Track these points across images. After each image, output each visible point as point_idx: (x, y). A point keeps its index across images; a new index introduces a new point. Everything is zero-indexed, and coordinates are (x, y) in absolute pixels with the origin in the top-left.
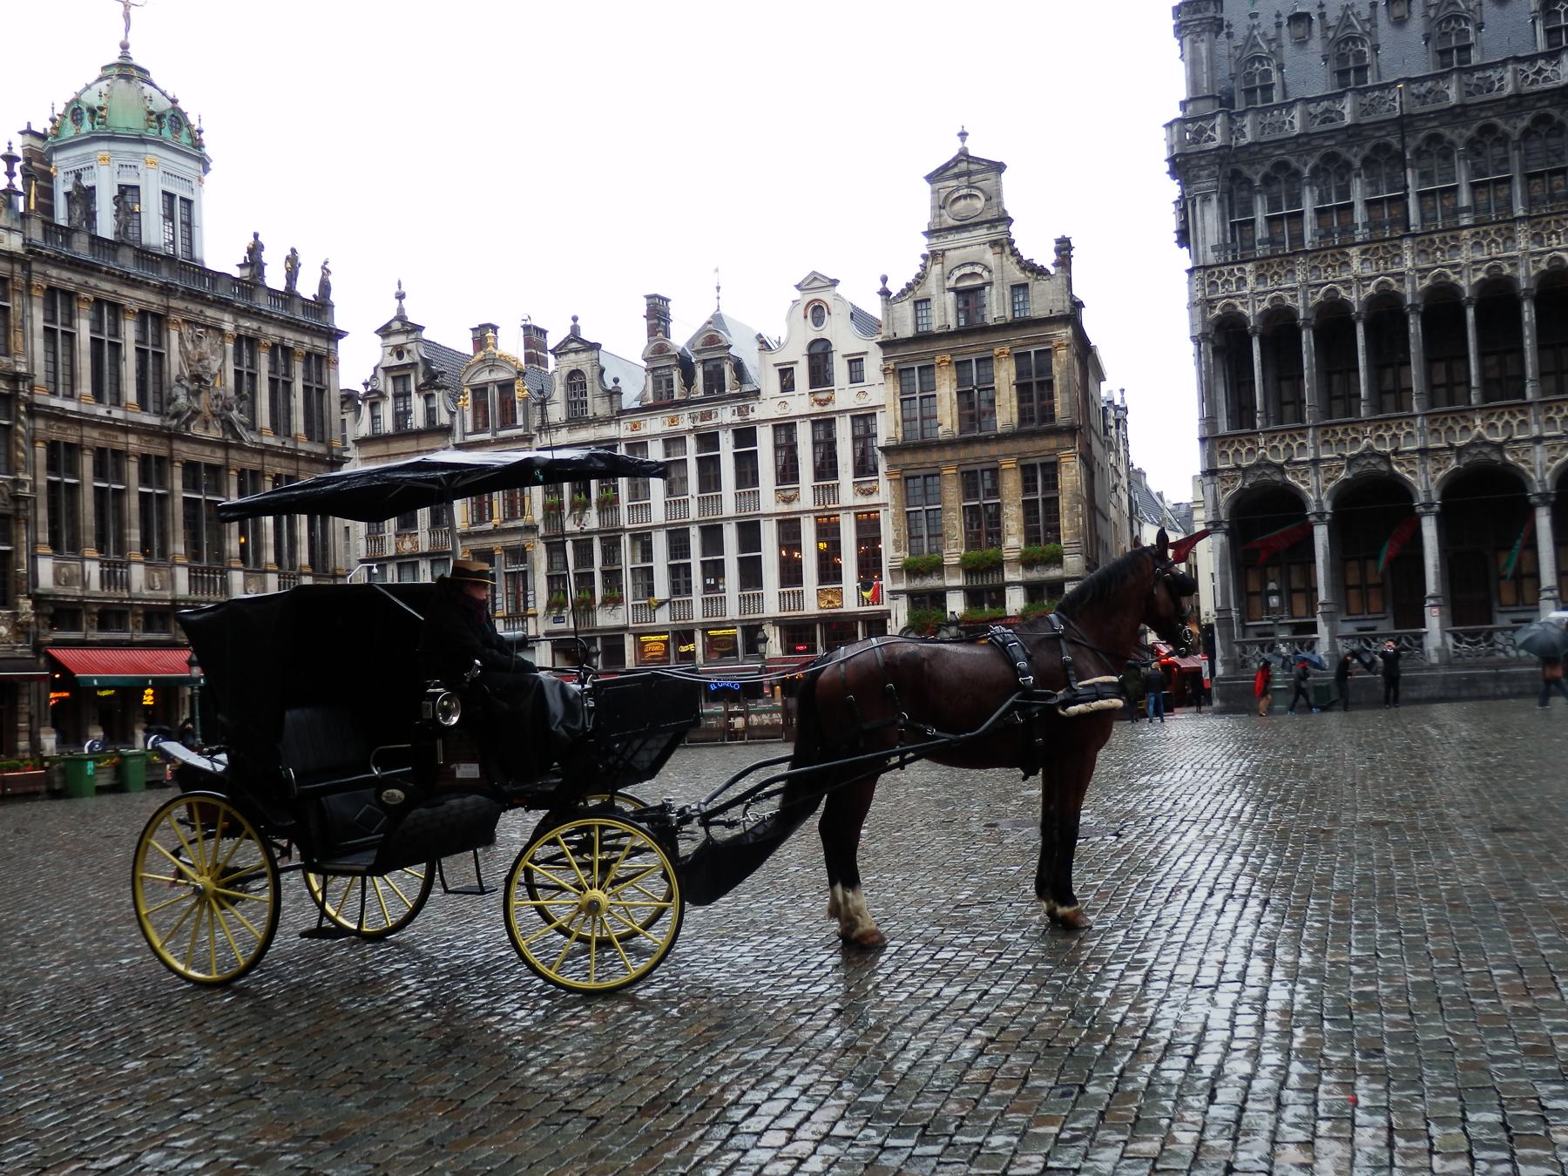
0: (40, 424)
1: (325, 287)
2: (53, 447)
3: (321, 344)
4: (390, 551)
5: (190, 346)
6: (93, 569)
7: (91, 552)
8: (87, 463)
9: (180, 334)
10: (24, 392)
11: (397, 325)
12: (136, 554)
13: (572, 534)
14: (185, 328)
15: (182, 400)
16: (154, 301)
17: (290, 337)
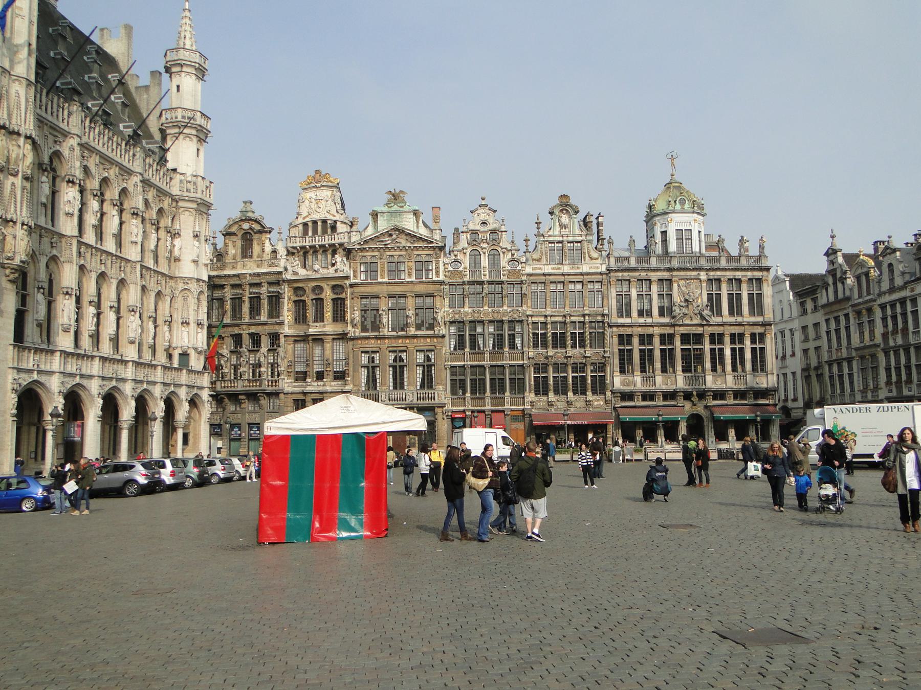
0: (615, 329)
1: (762, 247)
2: (621, 337)
3: (758, 274)
4: (834, 357)
5: (684, 289)
7: (638, 373)
8: (636, 340)
9: (679, 285)
10: (606, 320)
11: (830, 251)
12: (658, 372)
13: (891, 348)
14: (682, 282)
15: (678, 311)
16: (666, 275)
17: (739, 274)
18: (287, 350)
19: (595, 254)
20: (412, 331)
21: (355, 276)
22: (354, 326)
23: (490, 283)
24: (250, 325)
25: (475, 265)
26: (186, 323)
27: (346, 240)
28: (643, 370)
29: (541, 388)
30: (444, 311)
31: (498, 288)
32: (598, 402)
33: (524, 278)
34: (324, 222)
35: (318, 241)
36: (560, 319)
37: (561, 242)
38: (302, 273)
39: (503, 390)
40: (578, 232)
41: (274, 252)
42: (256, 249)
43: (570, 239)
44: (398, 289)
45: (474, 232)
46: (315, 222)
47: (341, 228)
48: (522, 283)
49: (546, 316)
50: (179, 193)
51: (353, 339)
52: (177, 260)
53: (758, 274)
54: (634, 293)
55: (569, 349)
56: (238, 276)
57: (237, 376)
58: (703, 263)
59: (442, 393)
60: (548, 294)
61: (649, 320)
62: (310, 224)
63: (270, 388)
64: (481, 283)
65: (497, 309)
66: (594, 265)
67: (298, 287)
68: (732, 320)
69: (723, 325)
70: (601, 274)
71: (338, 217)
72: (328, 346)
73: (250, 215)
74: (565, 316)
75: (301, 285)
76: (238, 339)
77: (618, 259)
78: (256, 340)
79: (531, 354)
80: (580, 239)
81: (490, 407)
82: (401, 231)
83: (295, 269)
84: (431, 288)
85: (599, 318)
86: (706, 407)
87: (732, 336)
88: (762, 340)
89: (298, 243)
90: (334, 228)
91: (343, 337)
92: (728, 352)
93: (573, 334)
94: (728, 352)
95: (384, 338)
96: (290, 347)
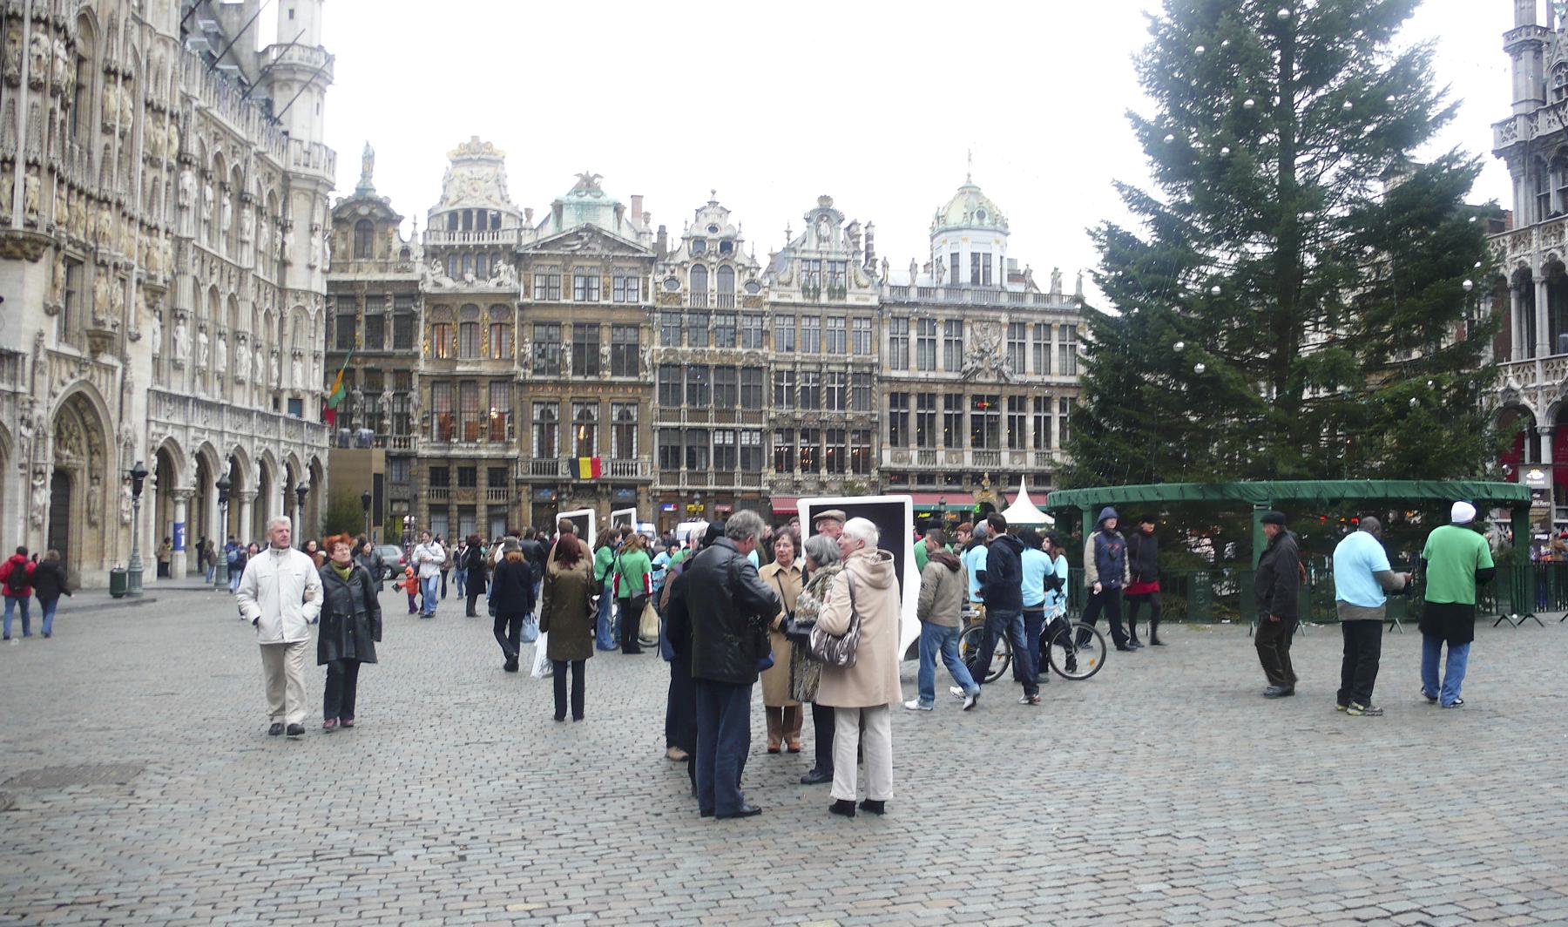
0: (886, 385)
2: (893, 396)
6: (914, 454)
7: (913, 445)
8: (913, 402)
10: (876, 372)
12: (940, 445)
14: (977, 326)
16: (956, 314)
18: (419, 395)
19: (863, 281)
20: (607, 376)
21: (527, 294)
22: (525, 366)
23: (719, 313)
24: (367, 357)
25: (699, 289)
26: (296, 356)
27: (514, 241)
28: (921, 442)
29: (784, 462)
30: (653, 349)
31: (730, 321)
33: (766, 308)
35: (472, 241)
36: (813, 368)
37: (819, 261)
38: (448, 284)
39: (732, 465)
40: (842, 248)
41: (406, 252)
42: (378, 245)
43: (832, 257)
44: (590, 316)
45: (699, 241)
46: (468, 212)
47: (507, 223)
48: (762, 315)
49: (795, 364)
50: (292, 168)
51: (524, 384)
54: (913, 336)
55: (824, 410)
58: (1004, 300)
59: (647, 465)
60: (798, 332)
62: (460, 214)
63: (397, 450)
64: (708, 313)
65: (725, 350)
67: (437, 303)
68: (1038, 379)
70: (871, 307)
71: (503, 207)
72: (484, 392)
73: (369, 194)
74: (821, 364)
75: (447, 302)
77: (893, 288)
79: (772, 415)
80: (844, 257)
81: (713, 487)
82: (594, 232)
83: (434, 279)
84: (635, 317)
85: (867, 369)
86: (1000, 494)
87: (1037, 400)
89: (443, 241)
90: (496, 222)
91: (505, 380)
92: (1030, 422)
93: (831, 390)
94: (1030, 422)
96: (427, 392)
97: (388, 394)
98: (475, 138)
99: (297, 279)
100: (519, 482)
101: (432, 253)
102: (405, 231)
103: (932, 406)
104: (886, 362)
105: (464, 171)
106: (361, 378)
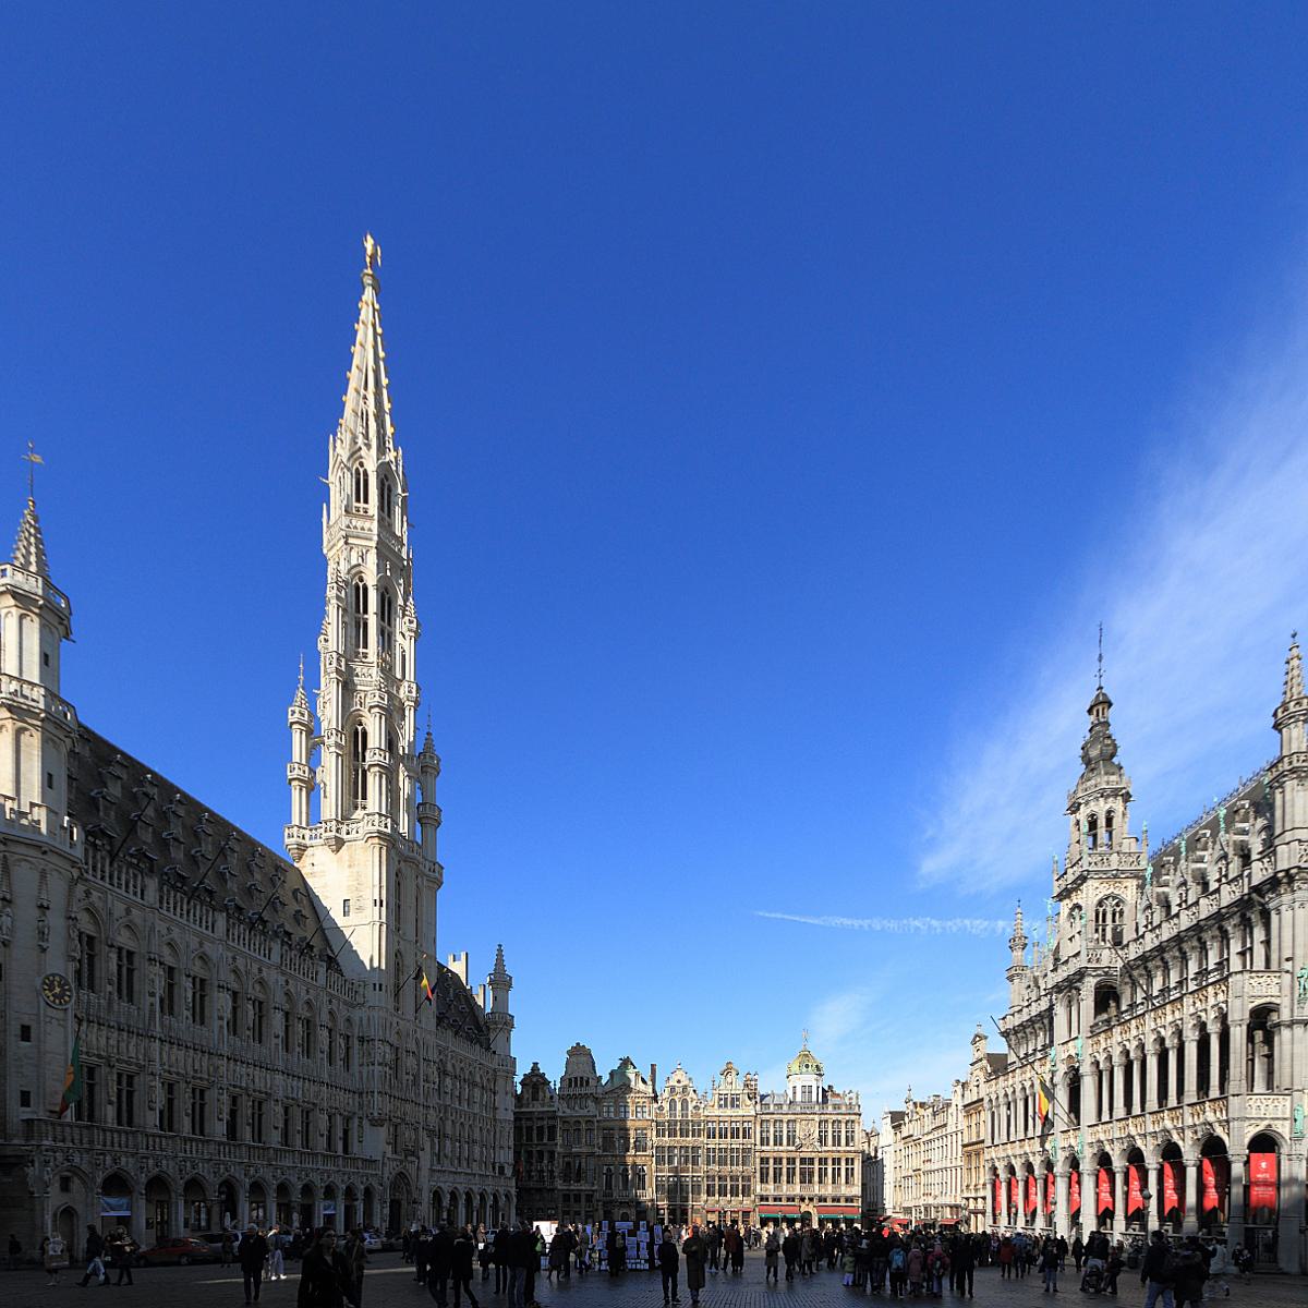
2: (762, 1159)
3: (853, 1117)
16: (793, 1117)
17: (840, 1118)
19: (748, 1102)
29: (710, 1193)
32: (747, 1203)
34: (582, 1078)
41: (552, 1097)
46: (576, 1078)
51: (599, 1156)
52: (496, 1109)
53: (853, 1117)
56: (531, 1112)
57: (530, 1177)
61: (781, 1148)
66: (748, 1109)
68: (834, 1148)
69: (828, 1151)
71: (590, 1076)
76: (530, 1154)
78: (541, 1153)
83: (562, 1109)
88: (852, 1164)
90: (587, 1082)
95: (616, 1156)
96: (561, 1160)
97: (546, 1162)
98: (578, 1044)
99: (501, 1115)
100: (598, 1201)
101: (561, 1097)
102: (552, 1085)
103: (781, 1163)
104: (758, 1142)
105: (574, 1059)
106: (535, 1155)
